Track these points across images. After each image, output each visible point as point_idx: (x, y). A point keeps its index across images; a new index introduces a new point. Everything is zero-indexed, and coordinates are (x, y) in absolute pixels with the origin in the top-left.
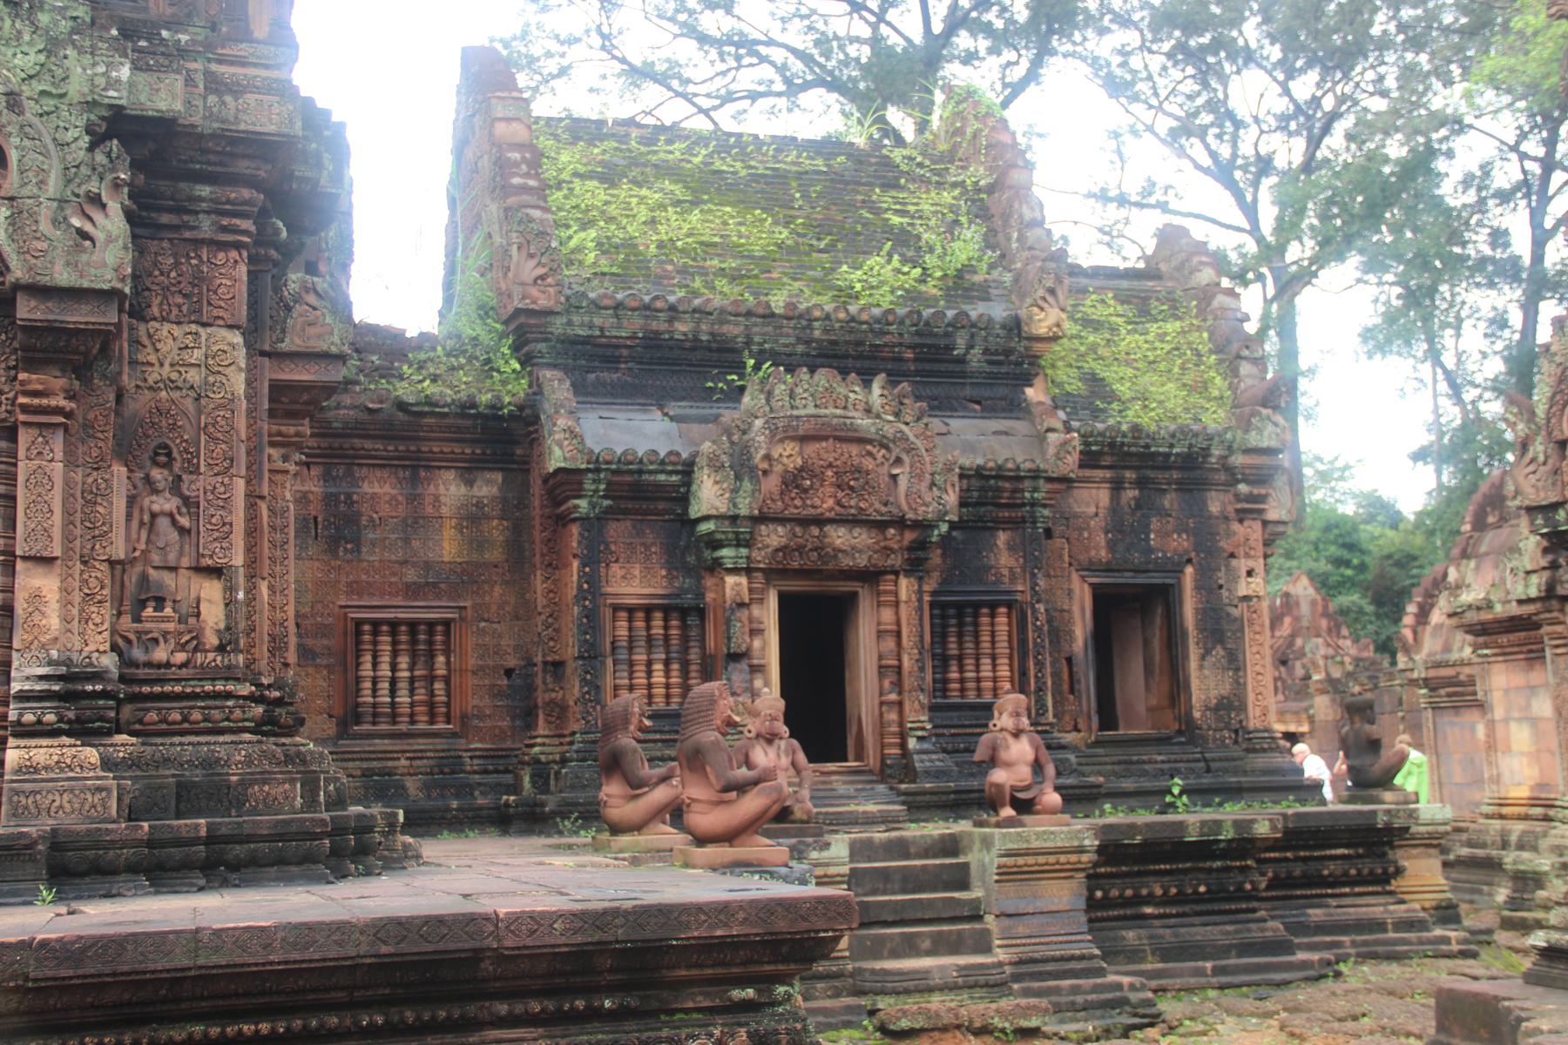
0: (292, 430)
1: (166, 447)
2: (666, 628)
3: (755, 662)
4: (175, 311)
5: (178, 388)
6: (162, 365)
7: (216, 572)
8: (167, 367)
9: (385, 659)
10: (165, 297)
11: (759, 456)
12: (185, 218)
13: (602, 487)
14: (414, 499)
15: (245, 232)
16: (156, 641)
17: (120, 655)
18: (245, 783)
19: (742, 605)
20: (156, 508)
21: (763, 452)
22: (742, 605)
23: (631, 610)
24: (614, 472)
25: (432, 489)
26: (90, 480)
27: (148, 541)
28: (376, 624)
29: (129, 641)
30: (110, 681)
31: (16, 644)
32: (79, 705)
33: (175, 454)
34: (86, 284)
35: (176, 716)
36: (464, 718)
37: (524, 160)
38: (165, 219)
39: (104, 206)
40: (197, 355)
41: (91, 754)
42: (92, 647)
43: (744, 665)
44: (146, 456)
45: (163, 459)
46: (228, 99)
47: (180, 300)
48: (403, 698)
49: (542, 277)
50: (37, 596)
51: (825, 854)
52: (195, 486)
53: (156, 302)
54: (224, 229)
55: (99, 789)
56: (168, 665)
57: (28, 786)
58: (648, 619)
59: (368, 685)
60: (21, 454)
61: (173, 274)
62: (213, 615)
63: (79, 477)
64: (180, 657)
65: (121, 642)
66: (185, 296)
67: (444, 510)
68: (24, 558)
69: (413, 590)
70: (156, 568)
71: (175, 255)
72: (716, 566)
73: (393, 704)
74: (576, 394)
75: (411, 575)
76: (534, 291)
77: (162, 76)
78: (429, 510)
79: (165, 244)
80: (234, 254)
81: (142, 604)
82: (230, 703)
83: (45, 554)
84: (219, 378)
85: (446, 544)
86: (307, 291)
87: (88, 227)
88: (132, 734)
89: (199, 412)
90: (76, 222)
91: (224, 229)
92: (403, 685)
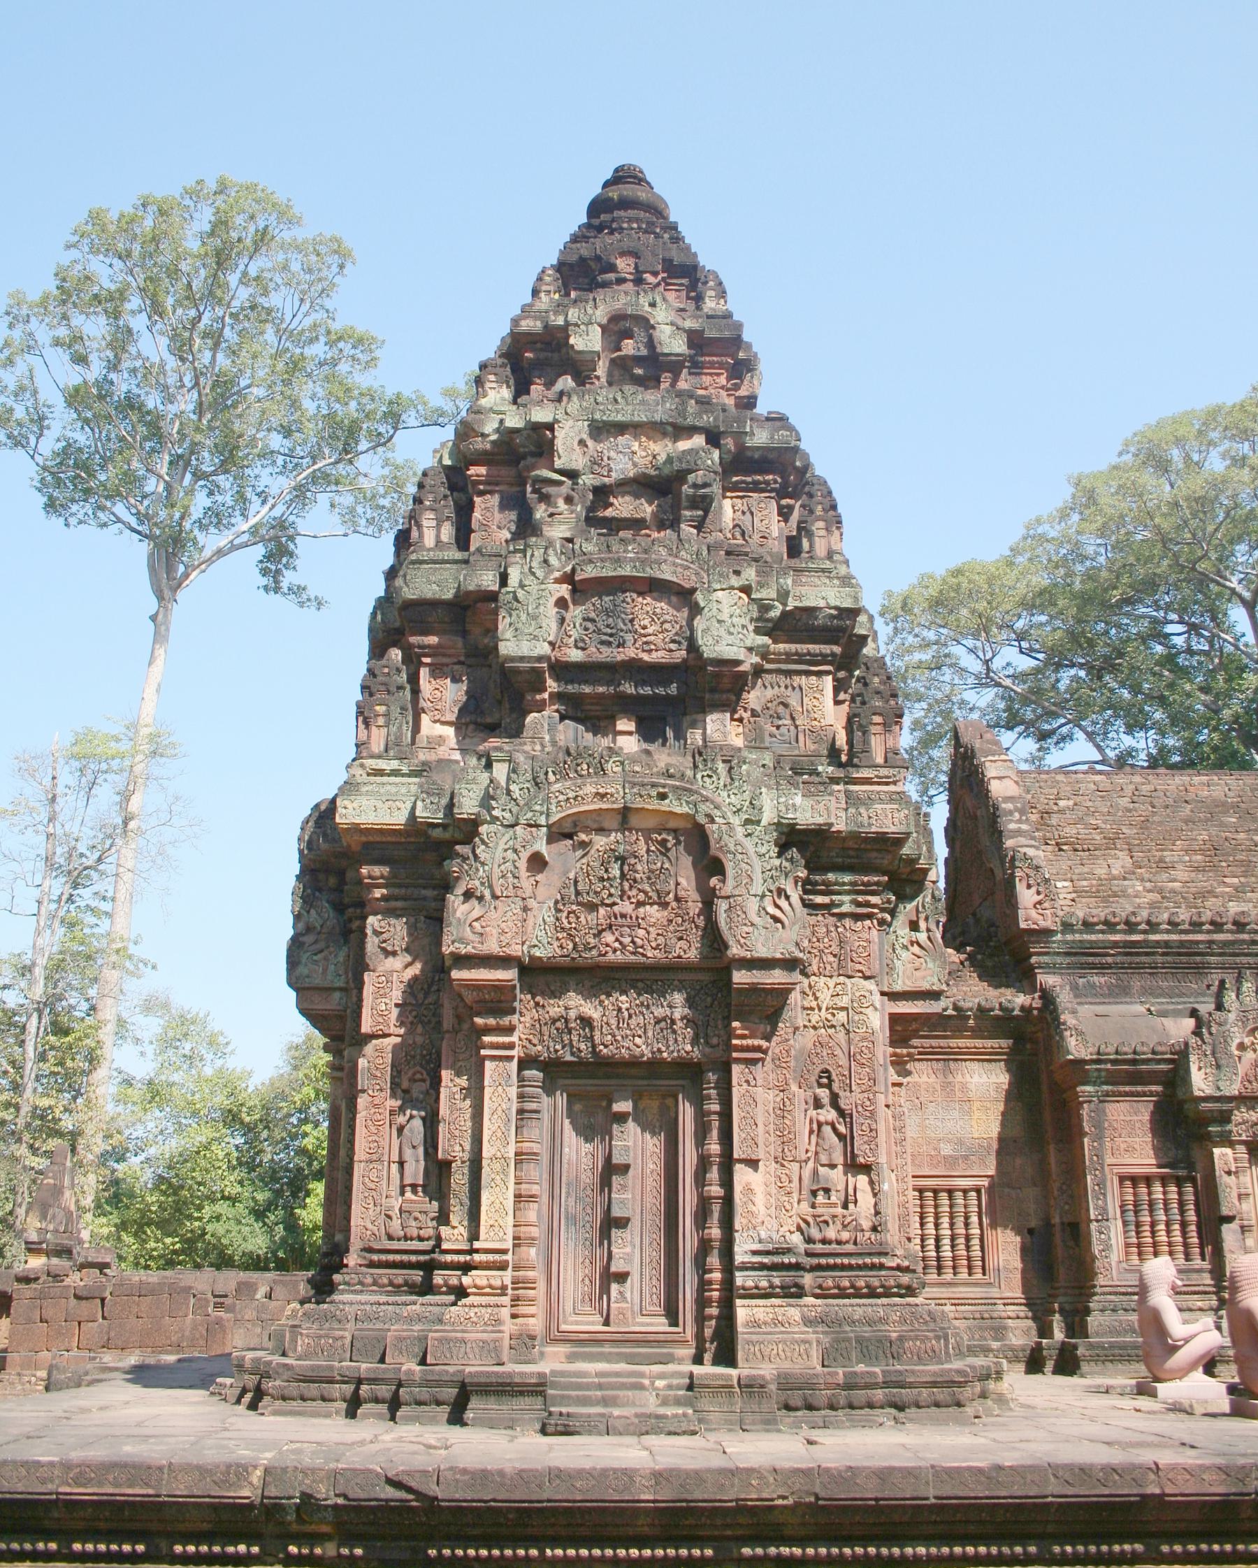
0: (905, 1051)
1: (827, 1071)
2: (1165, 1193)
3: (1246, 1223)
4: (828, 967)
5: (833, 1026)
6: (820, 1009)
7: (866, 1169)
8: (824, 1010)
10: (821, 957)
12: (834, 897)
14: (946, 1086)
15: (874, 906)
16: (826, 1222)
17: (802, 1234)
20: (822, 1119)
22: (1229, 1173)
23: (1134, 1180)
25: (959, 1078)
26: (778, 1099)
27: (817, 1144)
29: (808, 1223)
30: (800, 1254)
31: (737, 1226)
32: (787, 1274)
33: (834, 1077)
34: (778, 956)
38: (819, 899)
39: (787, 898)
41: (794, 1313)
42: (785, 1228)
43: (1234, 1226)
44: (813, 1079)
45: (825, 1081)
46: (862, 810)
47: (831, 959)
49: (1040, 903)
50: (749, 1190)
53: (815, 962)
54: (859, 904)
55: (805, 1342)
56: (839, 1243)
57: (754, 1337)
60: (734, 1082)
61: (826, 940)
63: (771, 1098)
65: (803, 1225)
66: (835, 956)
68: (740, 1161)
70: (823, 1165)
71: (826, 926)
72: (1207, 1141)
74: (1076, 996)
76: (1033, 913)
77: (820, 799)
79: (820, 918)
80: (868, 923)
81: (814, 1193)
82: (883, 1273)
83: (754, 1157)
86: (912, 943)
87: (778, 913)
88: (817, 1296)
89: (849, 1042)
90: (771, 910)
91: (859, 904)
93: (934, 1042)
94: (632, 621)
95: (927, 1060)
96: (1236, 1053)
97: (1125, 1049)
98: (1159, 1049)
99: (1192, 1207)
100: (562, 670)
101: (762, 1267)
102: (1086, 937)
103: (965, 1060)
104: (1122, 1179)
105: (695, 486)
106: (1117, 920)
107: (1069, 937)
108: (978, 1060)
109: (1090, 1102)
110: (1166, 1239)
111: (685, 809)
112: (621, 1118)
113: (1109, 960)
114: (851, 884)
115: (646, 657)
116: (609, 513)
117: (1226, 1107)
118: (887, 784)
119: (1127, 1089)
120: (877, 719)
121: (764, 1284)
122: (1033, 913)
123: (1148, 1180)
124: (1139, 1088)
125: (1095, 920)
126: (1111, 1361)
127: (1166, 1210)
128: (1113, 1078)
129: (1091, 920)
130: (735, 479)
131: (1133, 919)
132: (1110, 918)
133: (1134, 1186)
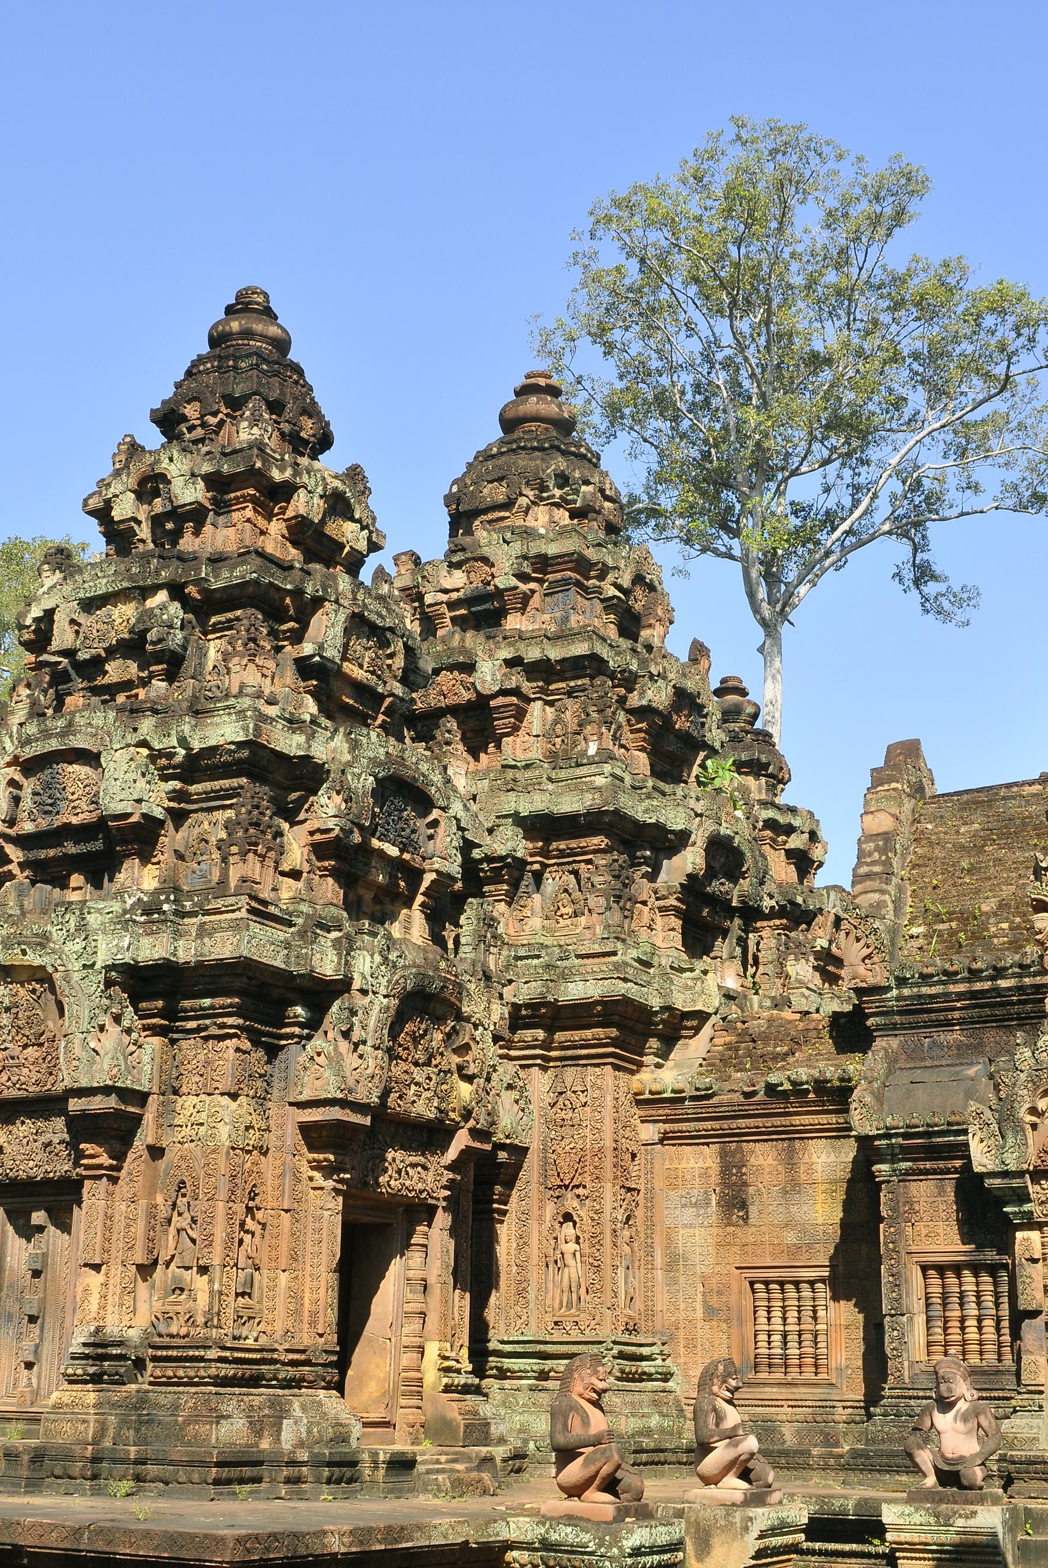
1: (184, 1183)
2: (977, 1284)
9: (777, 1313)
11: (1023, 1109)
13: (897, 1151)
18: (188, 1422)
19: (1035, 1261)
21: (1027, 1106)
22: (1035, 1261)
23: (941, 1269)
24: (906, 1136)
28: (767, 1283)
34: (95, 1085)
35: (170, 1373)
36: (840, 1369)
37: (877, 849)
38: (192, 1025)
40: (204, 1115)
47: (197, 1078)
48: (793, 1351)
49: (869, 956)
51: (972, 1522)
52: (200, 1206)
55: (84, 1421)
58: (959, 1276)
59: (763, 1337)
62: (203, 1300)
64: (183, 1331)
67: (819, 1176)
69: (795, 1250)
73: (785, 1357)
75: (790, 1238)
76: (861, 970)
78: (803, 1177)
84: (214, 1131)
85: (818, 1207)
90: (92, 1045)
92: (792, 1338)
93: (777, 1121)
94: (64, 789)
95: (772, 1140)
96: (1029, 1118)
97: (915, 1121)
98: (953, 1119)
99: (1006, 1299)
100: (23, 841)
101: (86, 1357)
102: (925, 990)
103: (812, 1138)
104: (924, 1269)
105: (153, 643)
106: (955, 968)
107: (906, 992)
108: (826, 1138)
109: (888, 1182)
110: (977, 1336)
111: (37, 962)
112: (41, 1229)
113: (957, 1015)
114: (212, 1007)
115: (75, 820)
116: (106, 680)
117: (1016, 1183)
118: (233, 911)
119: (928, 1165)
120: (234, 849)
121: (80, 1372)
122: (861, 970)
123: (957, 1269)
124: (941, 1164)
125: (930, 970)
126: (878, 1471)
127: (979, 1303)
128: (907, 1153)
129: (925, 971)
130: (213, 620)
131: (974, 966)
132: (947, 966)
133: (942, 1277)
